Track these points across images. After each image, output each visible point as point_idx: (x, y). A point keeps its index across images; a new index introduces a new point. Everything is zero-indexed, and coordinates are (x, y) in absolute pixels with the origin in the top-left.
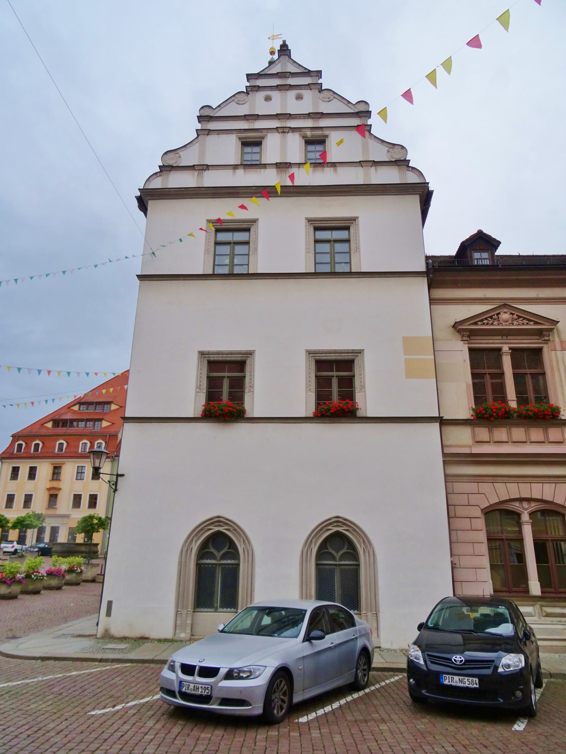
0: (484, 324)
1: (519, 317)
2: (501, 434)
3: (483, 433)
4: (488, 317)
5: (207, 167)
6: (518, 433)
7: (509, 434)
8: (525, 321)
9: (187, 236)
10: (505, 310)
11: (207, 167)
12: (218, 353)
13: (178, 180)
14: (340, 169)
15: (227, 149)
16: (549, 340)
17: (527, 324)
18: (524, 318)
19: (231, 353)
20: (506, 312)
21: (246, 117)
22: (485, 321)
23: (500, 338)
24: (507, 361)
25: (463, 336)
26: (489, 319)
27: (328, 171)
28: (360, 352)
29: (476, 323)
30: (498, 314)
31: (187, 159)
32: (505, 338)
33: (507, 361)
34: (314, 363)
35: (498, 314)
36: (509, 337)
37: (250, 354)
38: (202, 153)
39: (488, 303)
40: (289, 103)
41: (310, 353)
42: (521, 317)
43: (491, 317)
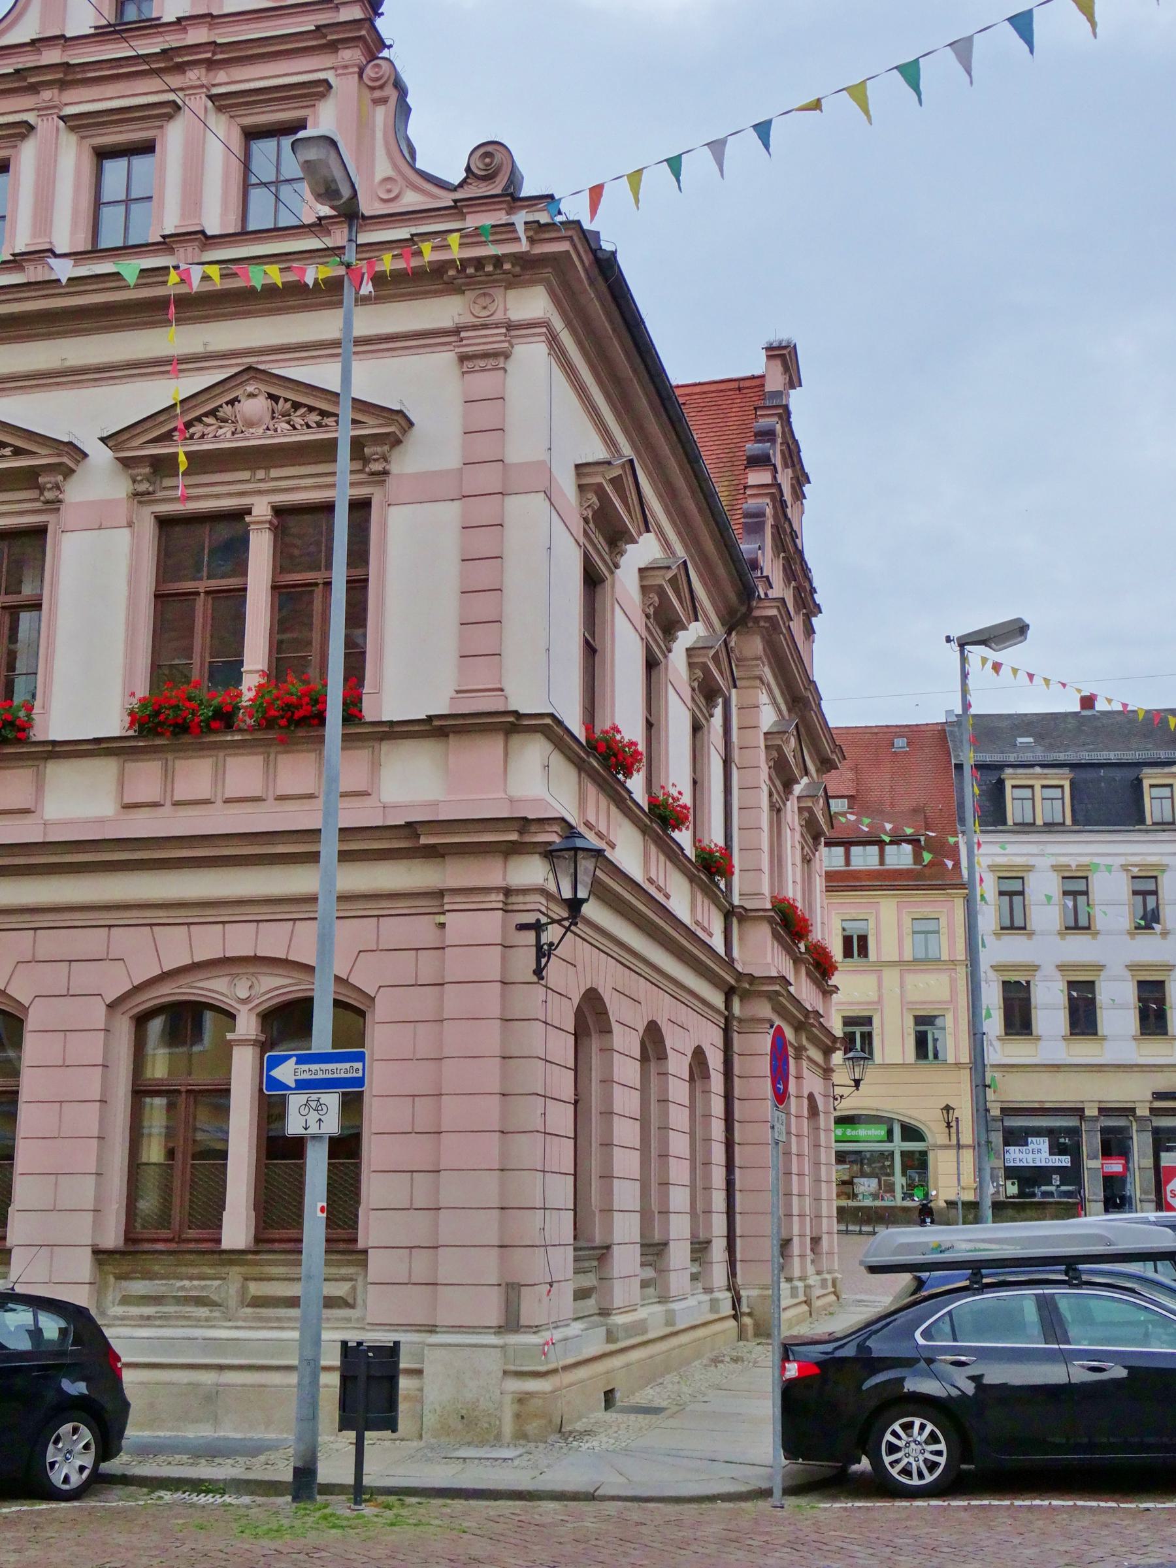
0: (192, 437)
1: (296, 406)
2: (195, 775)
3: (146, 777)
4: (206, 415)
6: (244, 772)
7: (219, 776)
8: (314, 418)
10: (250, 389)
16: (385, 473)
17: (319, 425)
18: (311, 409)
20: (251, 395)
22: (197, 429)
23: (246, 475)
24: (261, 550)
25: (134, 481)
26: (210, 420)
29: (167, 437)
30: (231, 402)
32: (261, 474)
33: (261, 550)
35: (231, 402)
36: (274, 473)
39: (224, 370)
42: (306, 406)
43: (213, 413)
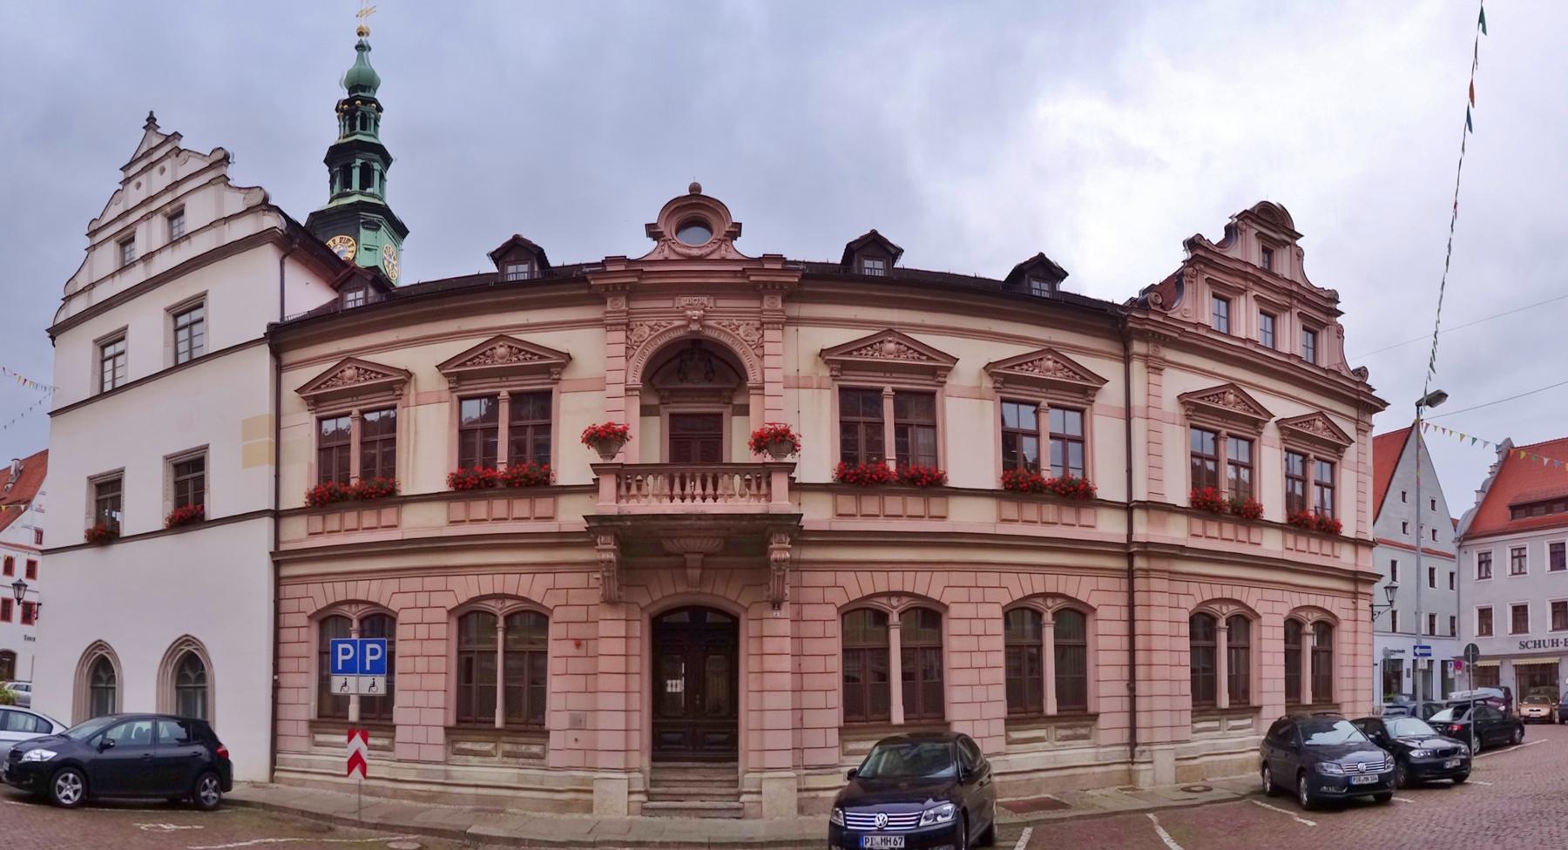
5: (93, 285)
9: (76, 363)
11: (93, 285)
12: (101, 476)
13: (78, 306)
14: (194, 239)
15: (108, 257)
19: (109, 473)
21: (120, 217)
27: (184, 244)
28: (206, 447)
31: (82, 282)
34: (171, 468)
37: (122, 471)
38: (91, 274)
40: (156, 181)
41: (167, 458)
